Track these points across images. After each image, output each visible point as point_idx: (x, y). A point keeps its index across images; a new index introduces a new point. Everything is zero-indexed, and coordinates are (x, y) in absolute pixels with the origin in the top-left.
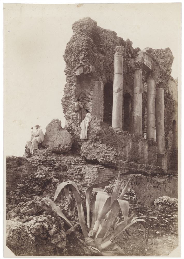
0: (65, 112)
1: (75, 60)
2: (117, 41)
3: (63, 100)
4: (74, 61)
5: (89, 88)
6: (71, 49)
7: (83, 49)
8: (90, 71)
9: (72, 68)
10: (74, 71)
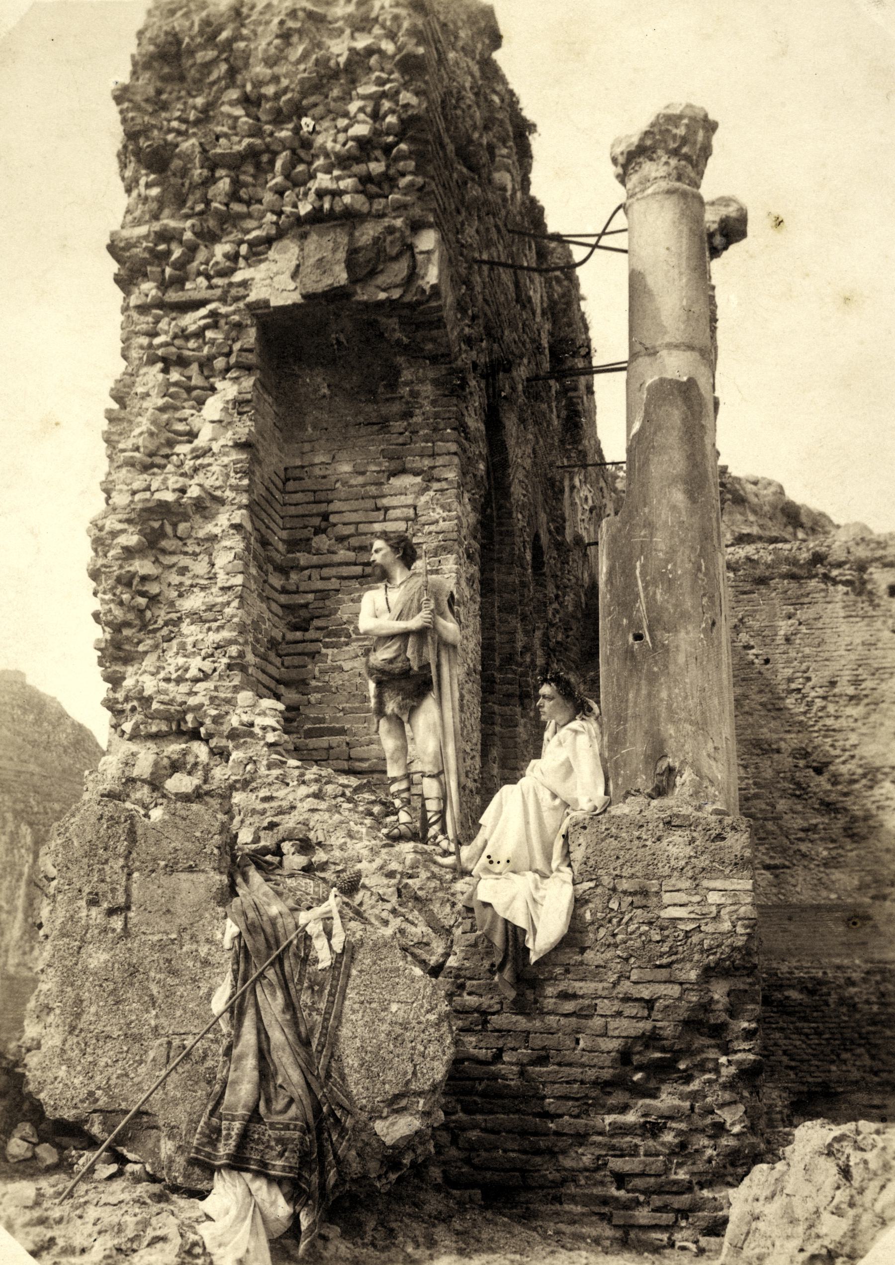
0: (115, 659)
1: (252, 154)
2: (496, 99)
6: (224, 35)
7: (370, 51)
9: (212, 223)
10: (234, 257)
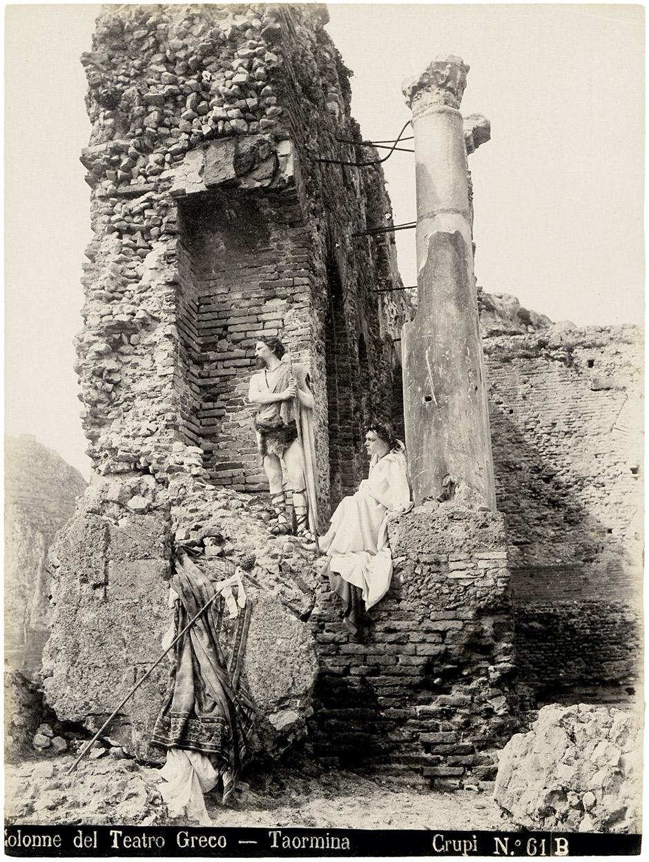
0: (93, 424)
1: (172, 96)
2: (327, 55)
3: (90, 344)
4: (166, 98)
5: (255, 283)
6: (151, 20)
7: (246, 28)
8: (277, 171)
9: (147, 141)
